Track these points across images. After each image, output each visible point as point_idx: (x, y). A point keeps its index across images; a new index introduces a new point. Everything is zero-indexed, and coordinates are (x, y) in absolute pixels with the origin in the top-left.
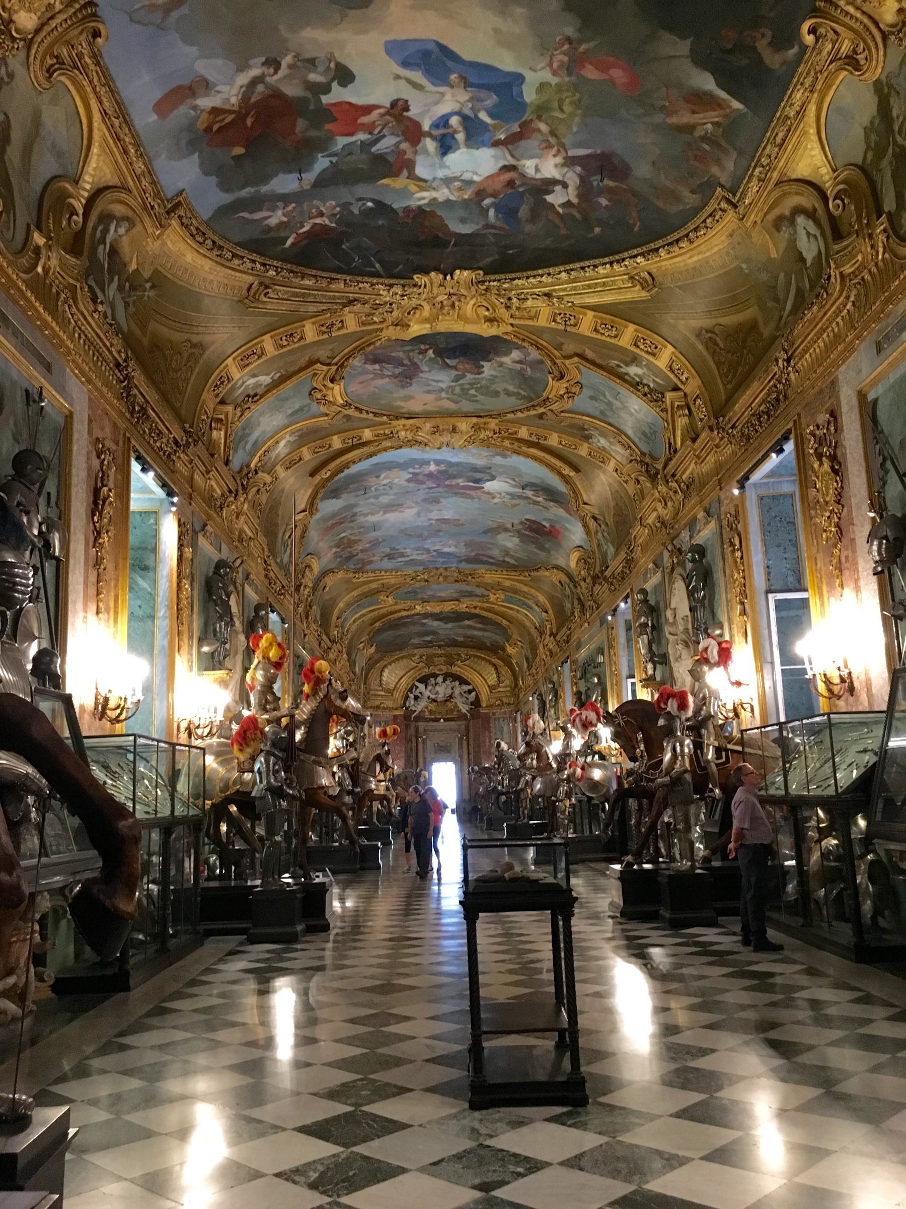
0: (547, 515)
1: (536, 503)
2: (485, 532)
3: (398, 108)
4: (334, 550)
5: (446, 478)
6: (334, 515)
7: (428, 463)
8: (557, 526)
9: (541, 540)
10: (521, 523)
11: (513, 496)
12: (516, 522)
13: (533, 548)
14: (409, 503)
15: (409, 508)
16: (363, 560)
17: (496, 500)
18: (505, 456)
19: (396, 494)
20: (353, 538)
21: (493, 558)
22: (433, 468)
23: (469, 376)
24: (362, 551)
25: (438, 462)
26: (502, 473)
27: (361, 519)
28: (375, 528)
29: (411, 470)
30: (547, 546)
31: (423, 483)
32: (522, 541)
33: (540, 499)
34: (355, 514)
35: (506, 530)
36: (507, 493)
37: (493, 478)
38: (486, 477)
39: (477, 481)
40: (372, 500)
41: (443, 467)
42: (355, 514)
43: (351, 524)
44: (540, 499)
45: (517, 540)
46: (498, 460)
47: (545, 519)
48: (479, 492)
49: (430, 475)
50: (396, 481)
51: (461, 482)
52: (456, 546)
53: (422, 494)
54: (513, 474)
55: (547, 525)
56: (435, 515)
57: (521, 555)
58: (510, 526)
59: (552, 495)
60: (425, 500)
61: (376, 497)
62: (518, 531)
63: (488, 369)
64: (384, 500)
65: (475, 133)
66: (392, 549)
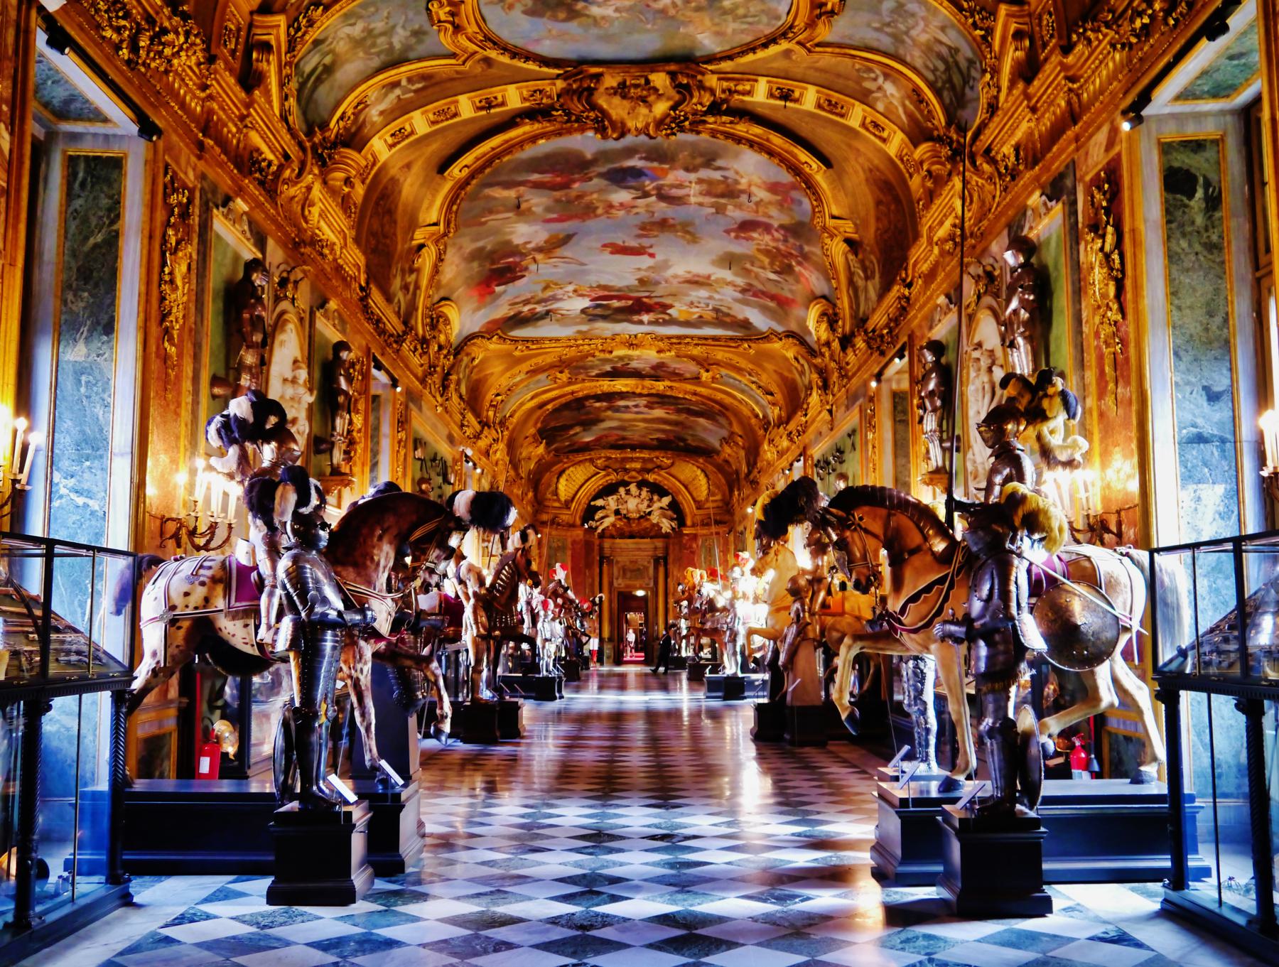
0: (505, 300)
1: (526, 302)
2: (567, 239)
3: (651, 408)
4: (797, 269)
5: (635, 307)
6: (764, 309)
7: (650, 323)
8: (488, 298)
9: (488, 266)
10: (526, 269)
11: (555, 299)
12: (533, 267)
13: (488, 243)
14: (675, 281)
15: (675, 276)
16: (781, 205)
17: (571, 288)
18: (579, 332)
19: (687, 295)
20: (766, 261)
21: (537, 186)
22: (645, 318)
23: (619, 365)
24: (767, 228)
25: (641, 322)
26: (576, 317)
27: (740, 281)
28: (729, 261)
29: (667, 317)
30: (475, 264)
31: (657, 304)
32: (509, 243)
33: (526, 309)
34: (743, 291)
35: (539, 250)
36: (561, 299)
37: (583, 311)
38: (590, 311)
39: (598, 306)
40: (717, 296)
41: (636, 318)
42: (743, 291)
43: (755, 283)
44: (526, 309)
45: (517, 240)
46: (584, 328)
47: (505, 292)
48: (594, 295)
49: (648, 309)
50: (685, 308)
51: (615, 303)
52: (611, 206)
53: (659, 291)
54: (564, 319)
55: (498, 289)
56: (644, 262)
57: (493, 221)
58: (539, 257)
59: (519, 320)
60: (657, 283)
61: (710, 298)
62: (523, 255)
63: (608, 368)
64: (703, 293)
65: (627, 407)
66: (720, 210)
